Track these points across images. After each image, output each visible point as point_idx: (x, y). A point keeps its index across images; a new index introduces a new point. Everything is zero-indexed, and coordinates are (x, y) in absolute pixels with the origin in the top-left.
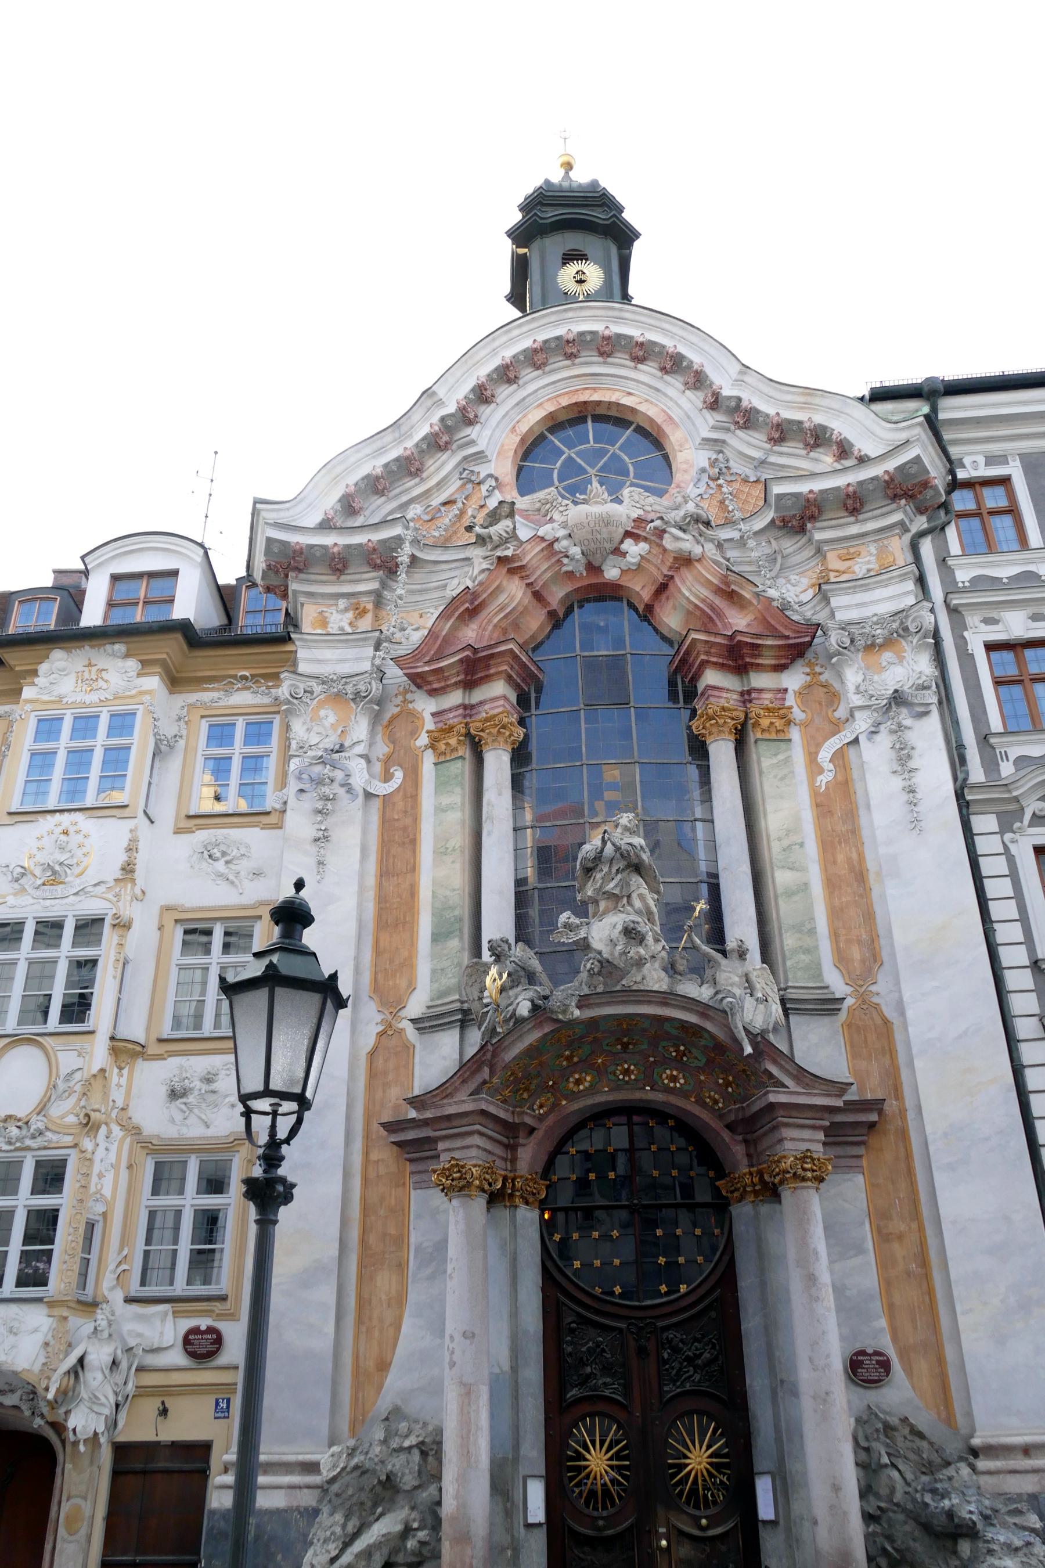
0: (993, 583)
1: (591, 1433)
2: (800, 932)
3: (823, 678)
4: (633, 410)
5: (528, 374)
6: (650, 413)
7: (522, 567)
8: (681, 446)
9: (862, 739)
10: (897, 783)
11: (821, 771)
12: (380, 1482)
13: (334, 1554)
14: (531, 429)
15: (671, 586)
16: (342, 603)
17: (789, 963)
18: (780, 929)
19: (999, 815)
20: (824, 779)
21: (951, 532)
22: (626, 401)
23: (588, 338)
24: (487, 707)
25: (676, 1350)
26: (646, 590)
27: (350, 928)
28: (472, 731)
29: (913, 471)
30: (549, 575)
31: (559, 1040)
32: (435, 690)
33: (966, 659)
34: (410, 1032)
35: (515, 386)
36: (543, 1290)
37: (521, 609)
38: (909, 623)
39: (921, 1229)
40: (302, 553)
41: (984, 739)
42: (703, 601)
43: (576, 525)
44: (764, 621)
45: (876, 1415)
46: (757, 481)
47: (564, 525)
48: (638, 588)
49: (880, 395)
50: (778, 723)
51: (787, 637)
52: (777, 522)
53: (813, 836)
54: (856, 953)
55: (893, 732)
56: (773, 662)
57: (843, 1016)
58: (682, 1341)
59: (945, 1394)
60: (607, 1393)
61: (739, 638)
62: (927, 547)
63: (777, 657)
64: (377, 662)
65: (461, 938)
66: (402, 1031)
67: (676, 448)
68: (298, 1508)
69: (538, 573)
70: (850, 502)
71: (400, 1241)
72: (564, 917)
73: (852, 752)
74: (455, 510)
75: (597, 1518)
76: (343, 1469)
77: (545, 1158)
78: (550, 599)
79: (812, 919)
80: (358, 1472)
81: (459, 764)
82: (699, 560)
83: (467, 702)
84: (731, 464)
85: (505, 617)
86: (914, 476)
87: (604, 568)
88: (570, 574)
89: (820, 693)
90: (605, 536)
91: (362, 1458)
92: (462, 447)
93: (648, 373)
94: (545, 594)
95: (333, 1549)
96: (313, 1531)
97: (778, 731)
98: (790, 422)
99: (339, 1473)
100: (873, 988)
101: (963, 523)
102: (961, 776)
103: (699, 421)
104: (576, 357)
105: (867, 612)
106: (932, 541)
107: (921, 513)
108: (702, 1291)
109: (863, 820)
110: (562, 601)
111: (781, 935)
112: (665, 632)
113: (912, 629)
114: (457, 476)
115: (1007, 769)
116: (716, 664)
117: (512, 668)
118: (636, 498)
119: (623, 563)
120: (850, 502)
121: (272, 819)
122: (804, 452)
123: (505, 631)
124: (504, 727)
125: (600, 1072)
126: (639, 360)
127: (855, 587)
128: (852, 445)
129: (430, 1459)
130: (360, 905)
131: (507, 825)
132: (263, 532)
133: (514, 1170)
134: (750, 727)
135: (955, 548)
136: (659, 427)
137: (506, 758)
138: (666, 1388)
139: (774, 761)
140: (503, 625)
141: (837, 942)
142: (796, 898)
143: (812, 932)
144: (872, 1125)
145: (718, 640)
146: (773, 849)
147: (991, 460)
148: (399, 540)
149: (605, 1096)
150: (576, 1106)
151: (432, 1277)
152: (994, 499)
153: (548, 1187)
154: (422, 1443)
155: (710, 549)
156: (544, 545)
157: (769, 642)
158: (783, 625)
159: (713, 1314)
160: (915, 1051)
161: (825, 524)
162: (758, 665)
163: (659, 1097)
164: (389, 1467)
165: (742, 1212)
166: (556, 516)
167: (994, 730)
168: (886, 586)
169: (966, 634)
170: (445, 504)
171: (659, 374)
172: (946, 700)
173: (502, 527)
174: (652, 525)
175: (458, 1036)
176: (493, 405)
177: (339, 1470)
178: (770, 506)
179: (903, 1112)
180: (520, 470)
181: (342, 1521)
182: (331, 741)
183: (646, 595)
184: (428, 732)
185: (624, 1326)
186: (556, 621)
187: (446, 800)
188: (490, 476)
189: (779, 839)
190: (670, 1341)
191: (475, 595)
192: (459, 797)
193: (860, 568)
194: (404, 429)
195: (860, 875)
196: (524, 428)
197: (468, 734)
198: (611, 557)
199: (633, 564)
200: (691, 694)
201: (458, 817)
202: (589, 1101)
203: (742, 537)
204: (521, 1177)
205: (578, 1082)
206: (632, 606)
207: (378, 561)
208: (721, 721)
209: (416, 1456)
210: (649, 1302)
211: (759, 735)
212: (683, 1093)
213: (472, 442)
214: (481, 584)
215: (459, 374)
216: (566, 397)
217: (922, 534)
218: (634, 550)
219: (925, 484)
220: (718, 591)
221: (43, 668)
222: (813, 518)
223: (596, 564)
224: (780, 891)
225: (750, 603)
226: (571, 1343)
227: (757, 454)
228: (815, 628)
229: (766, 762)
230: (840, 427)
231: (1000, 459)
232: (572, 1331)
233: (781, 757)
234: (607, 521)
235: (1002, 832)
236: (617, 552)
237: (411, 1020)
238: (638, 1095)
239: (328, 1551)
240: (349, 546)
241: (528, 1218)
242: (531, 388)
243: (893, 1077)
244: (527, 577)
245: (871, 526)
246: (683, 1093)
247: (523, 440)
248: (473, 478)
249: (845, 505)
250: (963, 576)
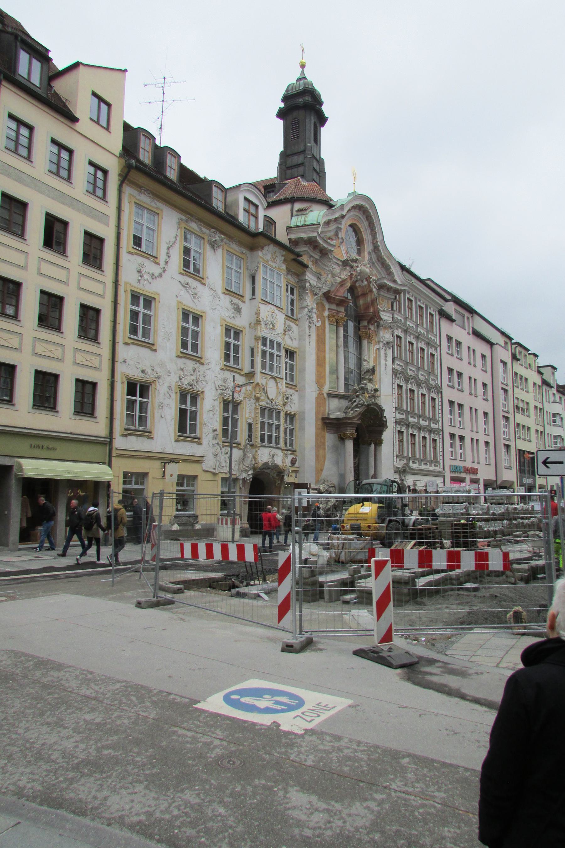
4: (361, 232)
16: (312, 259)
22: (361, 229)
34: (325, 395)
55: (385, 350)
71: (324, 443)
93: (366, 223)
121: (297, 322)
126: (367, 219)
148: (332, 251)
183: (360, 293)
188: (342, 238)
200: (359, 324)
218: (366, 283)
221: (266, 248)
230: (393, 269)
236: (362, 282)
245: (389, 296)
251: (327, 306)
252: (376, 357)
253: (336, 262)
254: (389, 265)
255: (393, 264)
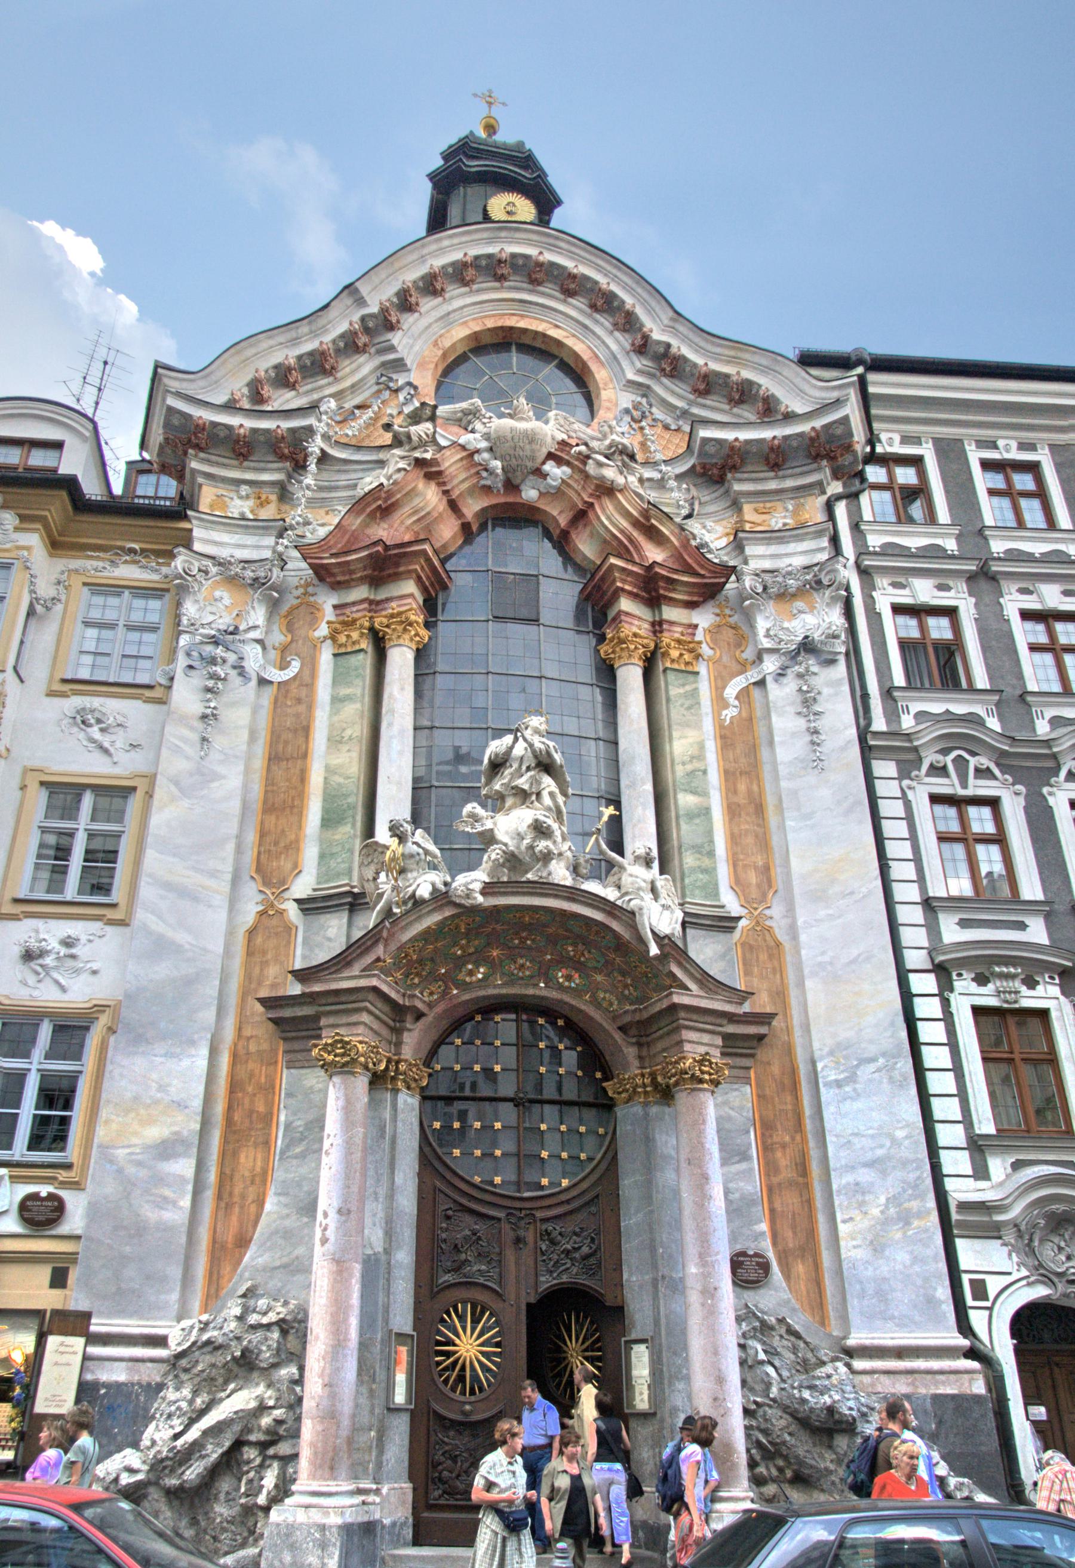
0: (903, 552)
1: (462, 1318)
2: (700, 853)
3: (732, 620)
4: (559, 343)
5: (454, 290)
6: (578, 347)
7: (440, 473)
8: (605, 384)
9: (769, 679)
10: (802, 723)
11: (726, 705)
12: (234, 1358)
13: (178, 1429)
14: (453, 346)
15: (591, 515)
17: (687, 881)
18: (680, 847)
19: (899, 762)
20: (729, 714)
21: (864, 499)
22: (553, 333)
23: (521, 262)
24: (394, 604)
25: (553, 1242)
26: (564, 515)
27: (235, 806)
28: (376, 626)
29: (839, 431)
30: (466, 485)
31: (457, 927)
32: (339, 583)
33: (874, 617)
35: (440, 299)
36: (420, 1175)
37: (435, 514)
38: (822, 576)
39: (804, 1140)
40: (204, 429)
41: (888, 693)
42: (622, 531)
43: (499, 438)
44: (678, 556)
45: (754, 1314)
46: (678, 430)
47: (487, 437)
48: (555, 513)
49: (809, 360)
50: (687, 657)
51: (703, 576)
52: (698, 468)
53: (715, 765)
54: (753, 878)
55: (800, 676)
56: (686, 598)
57: (737, 934)
58: (560, 1234)
59: (820, 1293)
60: (481, 1280)
61: (658, 570)
62: (841, 510)
63: (690, 594)
64: (280, 548)
65: (354, 825)
66: (281, 913)
67: (601, 386)
68: (139, 1384)
69: (456, 482)
70: (773, 456)
72: (468, 808)
73: (756, 693)
74: (370, 413)
75: (465, 1403)
76: (194, 1343)
77: (429, 1046)
78: (465, 510)
79: (711, 841)
80: (209, 1348)
81: (361, 656)
82: (620, 491)
83: (372, 597)
84: (654, 410)
85: (419, 520)
86: (839, 437)
87: (523, 487)
88: (487, 490)
89: (728, 634)
90: (528, 453)
91: (215, 1333)
92: (380, 352)
93: (575, 308)
94: (460, 504)
95: (178, 1425)
96: (156, 1405)
97: (687, 664)
98: (718, 374)
99: (190, 1347)
100: (767, 912)
101: (875, 494)
102: (862, 721)
103: (625, 364)
104: (506, 279)
105: (781, 564)
106: (847, 506)
107: (837, 479)
108: (585, 1185)
109: (764, 754)
110: (477, 515)
111: (680, 853)
112: (578, 560)
113: (826, 582)
114: (373, 381)
115: (907, 722)
116: (630, 593)
117: (422, 568)
118: (562, 422)
119: (542, 485)
120: (773, 456)
122: (727, 407)
123: (417, 533)
124: (411, 624)
125: (493, 966)
126: (569, 293)
127: (770, 538)
128: (777, 401)
129: (290, 1338)
130: (246, 788)
131: (409, 722)
132: (164, 400)
133: (398, 1053)
134: (659, 655)
135: (867, 515)
136: (584, 365)
137: (410, 656)
138: (543, 1279)
139: (681, 691)
140: (416, 528)
141: (735, 865)
142: (697, 821)
143: (711, 854)
144: (761, 1038)
145: (635, 569)
146: (677, 772)
147: (906, 440)
149: (499, 988)
150: (466, 997)
151: (303, 1156)
152: (906, 476)
153: (430, 1075)
154: (283, 1320)
155: (633, 480)
156: (464, 454)
157: (685, 579)
158: (699, 564)
159: (593, 1209)
160: (806, 972)
161: (746, 476)
162: (671, 599)
163: (554, 994)
164: (245, 1343)
165: (627, 1114)
166: (478, 426)
167: (896, 684)
168: (802, 540)
169: (874, 594)
170: (358, 407)
171: (588, 310)
172: (854, 654)
173: (423, 429)
174: (577, 449)
175: (345, 920)
176: (416, 315)
177: (188, 1344)
178: (692, 453)
179: (789, 1030)
180: (439, 385)
181: (190, 1396)
182: (225, 621)
183: (563, 521)
184: (328, 622)
185: (500, 1214)
186: (468, 533)
187: (344, 691)
188: (409, 384)
189: (684, 764)
190: (548, 1234)
191: (390, 494)
192: (361, 688)
193: (777, 521)
194: (321, 322)
195: (759, 809)
196: (447, 343)
197: (372, 629)
198: (531, 477)
199: (551, 486)
201: (356, 711)
202: (482, 993)
203: (662, 479)
204: (406, 1061)
205: (471, 973)
206: (547, 534)
207: (286, 451)
208: (632, 647)
209: (276, 1335)
210: (527, 1194)
211: (668, 665)
212: (577, 992)
213: (392, 349)
214: (395, 483)
215: (383, 276)
216: (492, 320)
217: (839, 497)
219: (848, 448)
220: (636, 523)
222: (734, 468)
223: (516, 482)
224: (681, 813)
225: (668, 540)
226: (447, 1230)
227: (680, 404)
228: (729, 571)
229: (674, 691)
230: (767, 384)
231: (917, 441)
232: (448, 1218)
233: (688, 688)
234: (531, 438)
235: (900, 778)
237: (295, 900)
238: (531, 991)
239: (172, 1427)
240: (254, 431)
241: (408, 1102)
242: (457, 304)
243: (780, 995)
244: (444, 484)
245: (789, 483)
246: (577, 992)
247: (444, 355)
248: (391, 384)
249: (767, 459)
250: (874, 541)
251: (327, 601)
252: (747, 722)
253: (374, 457)
254: (750, 383)
255: (765, 370)
